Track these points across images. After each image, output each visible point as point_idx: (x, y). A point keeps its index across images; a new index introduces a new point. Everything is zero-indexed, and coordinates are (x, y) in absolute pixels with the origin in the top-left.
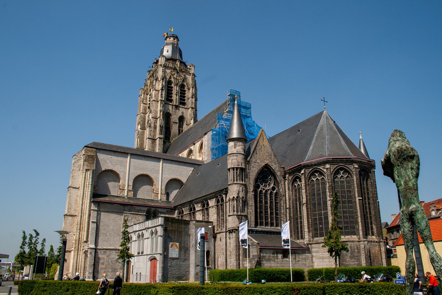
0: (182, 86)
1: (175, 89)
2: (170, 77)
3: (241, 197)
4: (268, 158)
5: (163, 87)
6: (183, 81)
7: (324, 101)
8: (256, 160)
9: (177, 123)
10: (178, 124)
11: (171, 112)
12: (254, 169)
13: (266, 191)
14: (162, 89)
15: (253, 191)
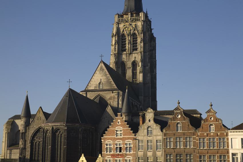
0: (135, 34)
1: (128, 39)
2: (123, 31)
3: (21, 147)
4: (42, 123)
5: (115, 43)
6: (134, 30)
7: (69, 82)
8: (33, 126)
9: (130, 68)
10: (131, 68)
11: (125, 60)
12: (32, 131)
13: (40, 142)
14: (115, 44)
15: (30, 143)
